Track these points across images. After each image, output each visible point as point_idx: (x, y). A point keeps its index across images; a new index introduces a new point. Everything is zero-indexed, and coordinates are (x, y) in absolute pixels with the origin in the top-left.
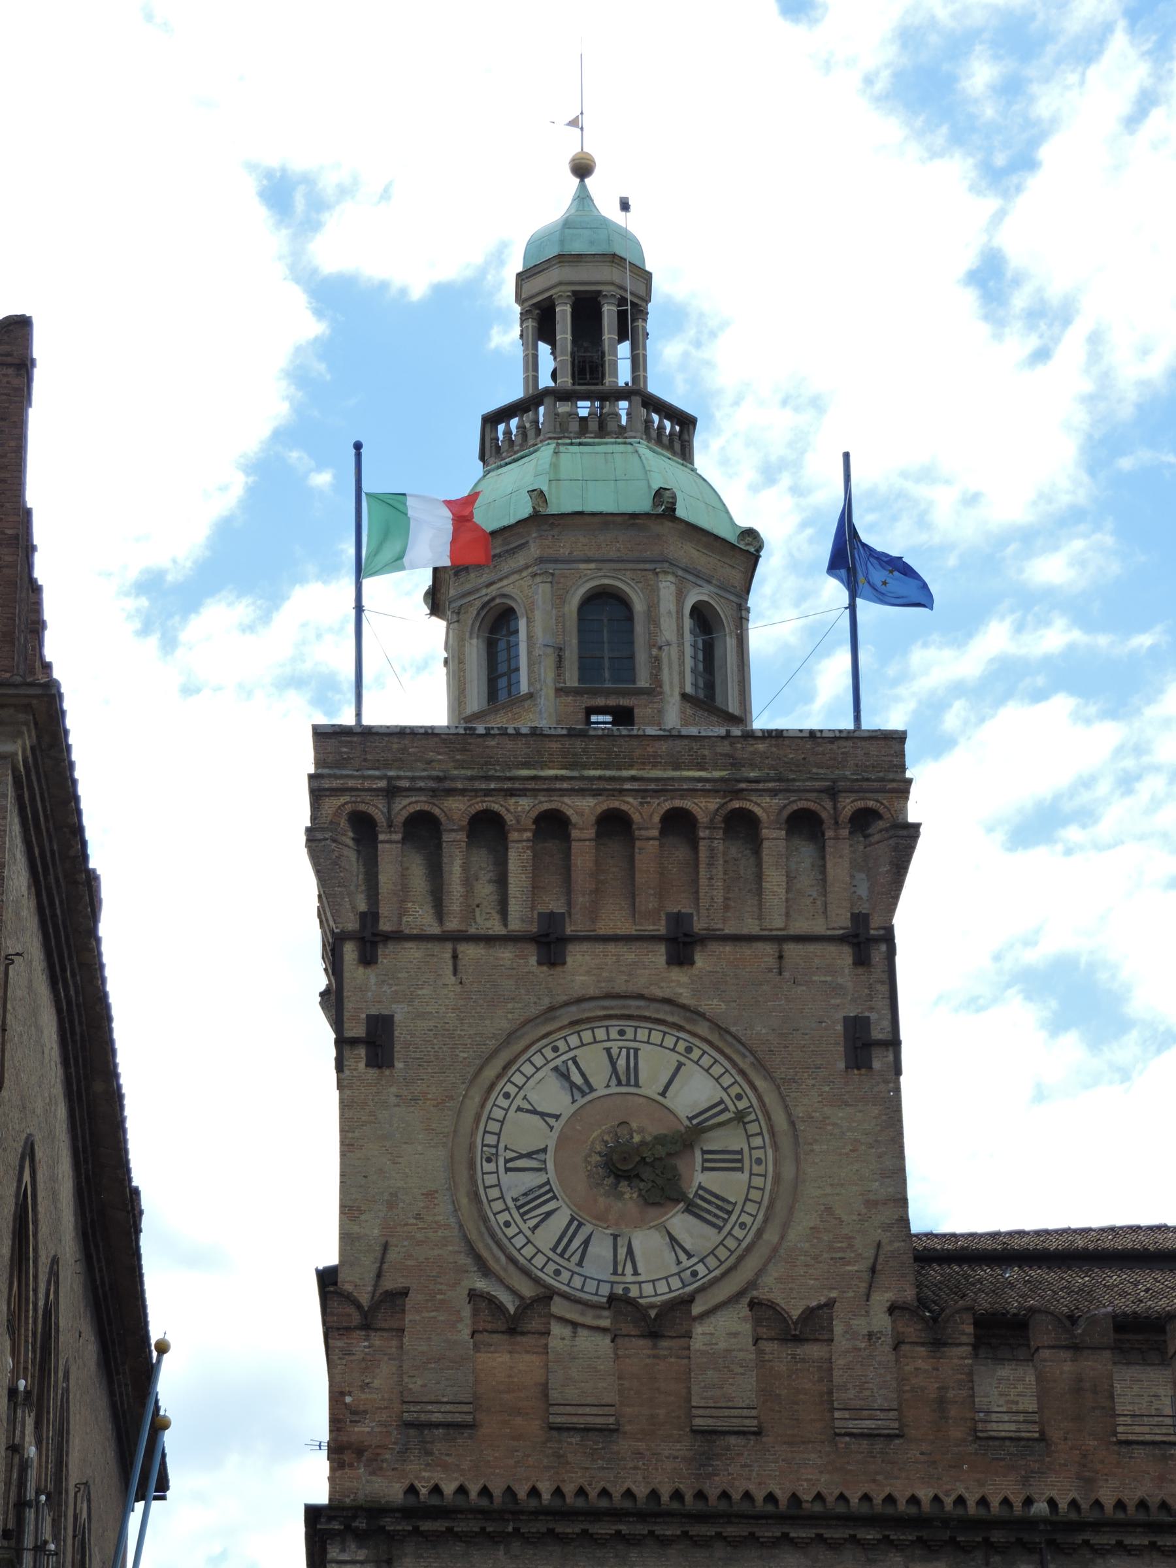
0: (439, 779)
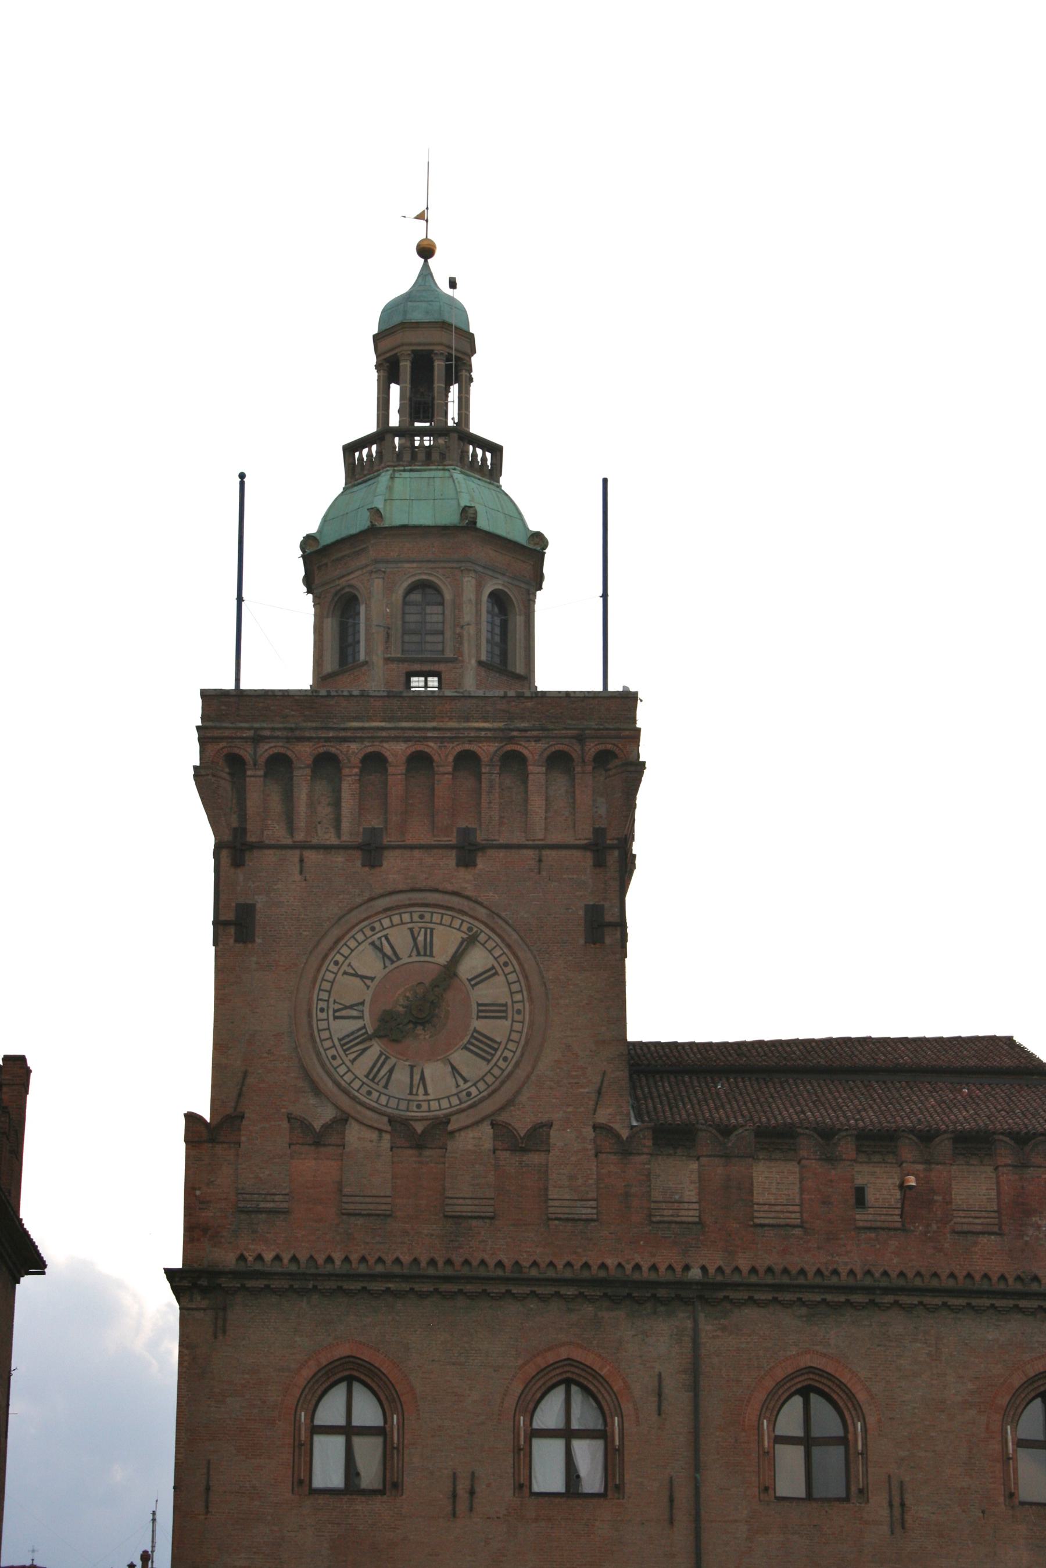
0: (292, 730)
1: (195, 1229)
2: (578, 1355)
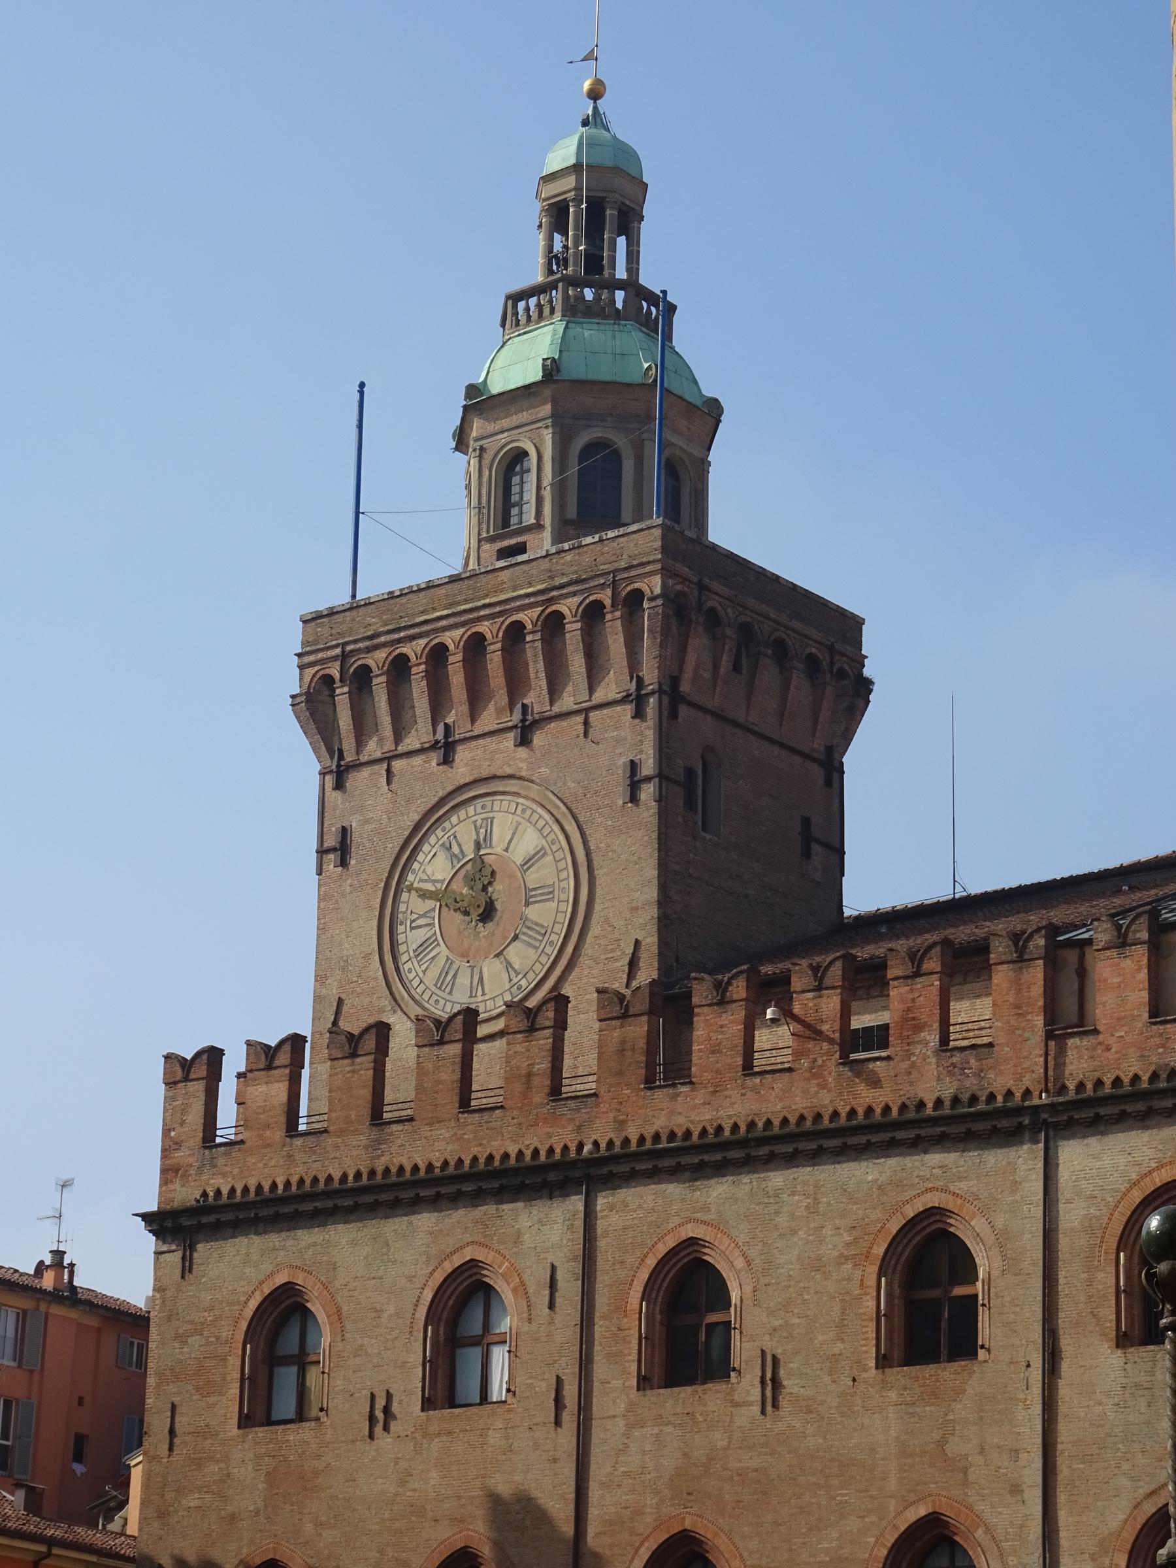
1: (169, 1172)
2: (481, 1255)
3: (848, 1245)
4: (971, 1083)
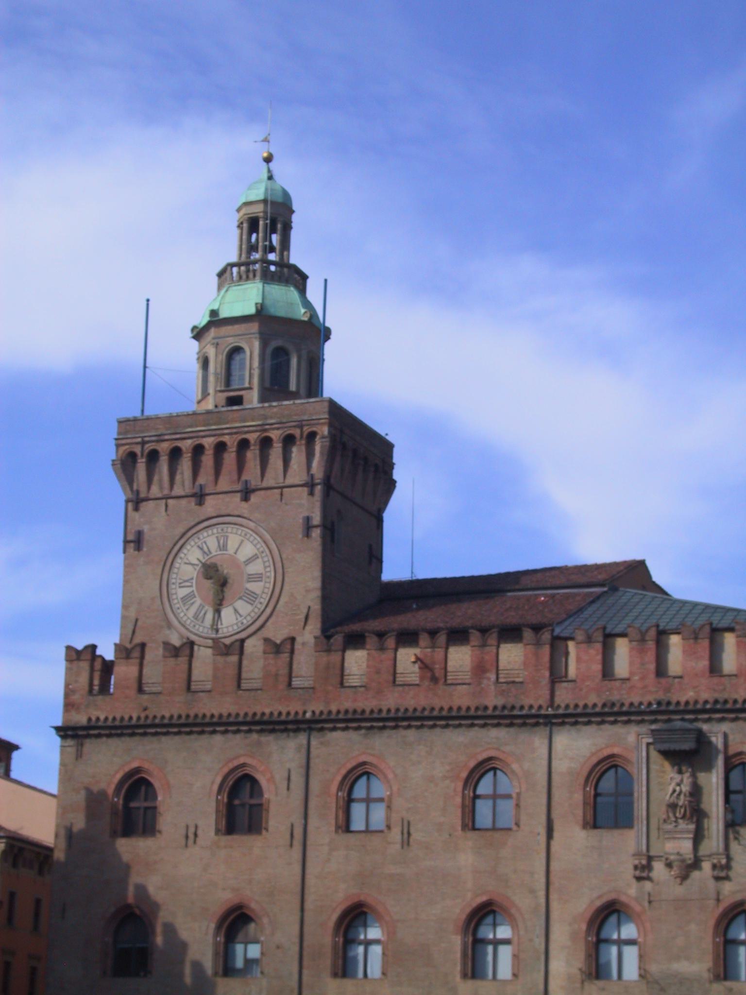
0: (159, 435)
1: (69, 705)
2: (249, 761)
3: (448, 771)
4: (511, 701)
